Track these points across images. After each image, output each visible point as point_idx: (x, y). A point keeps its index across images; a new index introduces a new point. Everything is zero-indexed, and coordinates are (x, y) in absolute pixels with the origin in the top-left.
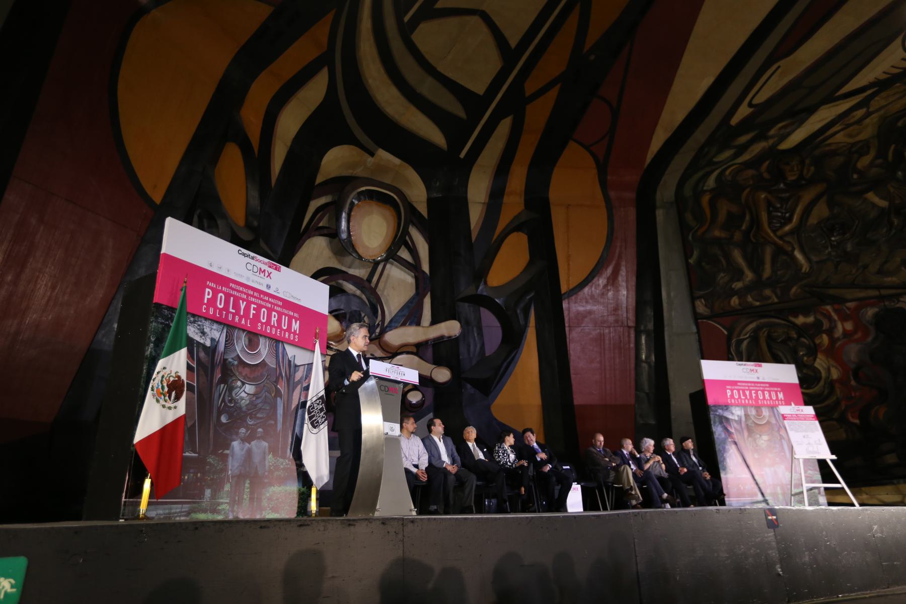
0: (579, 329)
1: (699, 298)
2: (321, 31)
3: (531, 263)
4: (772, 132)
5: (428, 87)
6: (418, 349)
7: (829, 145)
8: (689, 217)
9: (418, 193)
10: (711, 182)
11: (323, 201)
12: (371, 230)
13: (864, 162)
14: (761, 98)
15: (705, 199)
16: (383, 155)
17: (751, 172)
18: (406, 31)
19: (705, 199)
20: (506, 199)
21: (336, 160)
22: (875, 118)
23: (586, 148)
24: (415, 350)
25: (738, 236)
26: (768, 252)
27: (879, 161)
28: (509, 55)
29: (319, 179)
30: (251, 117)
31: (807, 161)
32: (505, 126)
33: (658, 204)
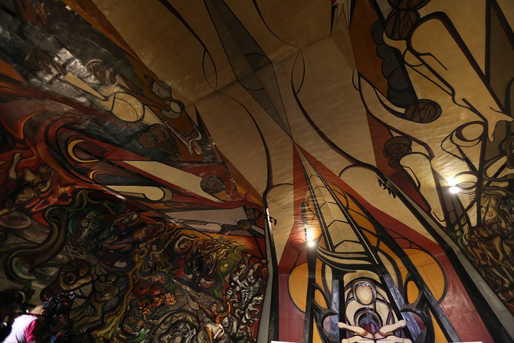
0: (452, 316)
1: (498, 292)
2: (318, 260)
3: (419, 292)
4: (462, 223)
5: (351, 256)
6: (394, 333)
7: (487, 221)
8: (469, 256)
9: (376, 277)
10: (466, 243)
11: (349, 290)
12: (365, 294)
13: (503, 225)
14: (442, 218)
15: (469, 248)
16: (358, 271)
17: (473, 236)
18: (333, 251)
19: (469, 248)
20: (401, 271)
21: (347, 278)
22: (490, 209)
23: (410, 248)
24: (392, 334)
25: (490, 264)
26: (504, 268)
27: (508, 224)
28: (361, 242)
29: (345, 285)
30: (319, 281)
31: (486, 228)
32: (379, 253)
33: (457, 254)
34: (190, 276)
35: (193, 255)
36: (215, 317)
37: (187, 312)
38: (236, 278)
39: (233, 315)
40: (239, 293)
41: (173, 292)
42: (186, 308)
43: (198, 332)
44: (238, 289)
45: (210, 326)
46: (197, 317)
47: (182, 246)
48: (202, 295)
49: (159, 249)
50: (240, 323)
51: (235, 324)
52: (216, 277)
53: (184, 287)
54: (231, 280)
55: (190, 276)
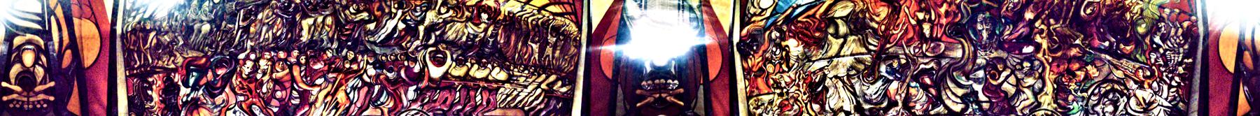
34: (1107, 44)
35: (1104, 18)
36: (1143, 82)
37: (1113, 81)
38: (1157, 39)
39: (1162, 79)
40: (1163, 55)
41: (1093, 63)
42: (1111, 77)
43: (1129, 99)
44: (1161, 51)
45: (1140, 93)
46: (1125, 85)
47: (1088, 11)
48: (1124, 61)
49: (1057, 22)
50: (1170, 87)
51: (1165, 87)
52: (1138, 41)
53: (1103, 56)
54: (1152, 42)
55: (1107, 44)
